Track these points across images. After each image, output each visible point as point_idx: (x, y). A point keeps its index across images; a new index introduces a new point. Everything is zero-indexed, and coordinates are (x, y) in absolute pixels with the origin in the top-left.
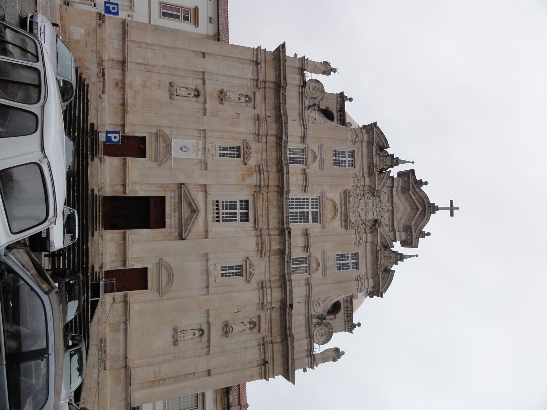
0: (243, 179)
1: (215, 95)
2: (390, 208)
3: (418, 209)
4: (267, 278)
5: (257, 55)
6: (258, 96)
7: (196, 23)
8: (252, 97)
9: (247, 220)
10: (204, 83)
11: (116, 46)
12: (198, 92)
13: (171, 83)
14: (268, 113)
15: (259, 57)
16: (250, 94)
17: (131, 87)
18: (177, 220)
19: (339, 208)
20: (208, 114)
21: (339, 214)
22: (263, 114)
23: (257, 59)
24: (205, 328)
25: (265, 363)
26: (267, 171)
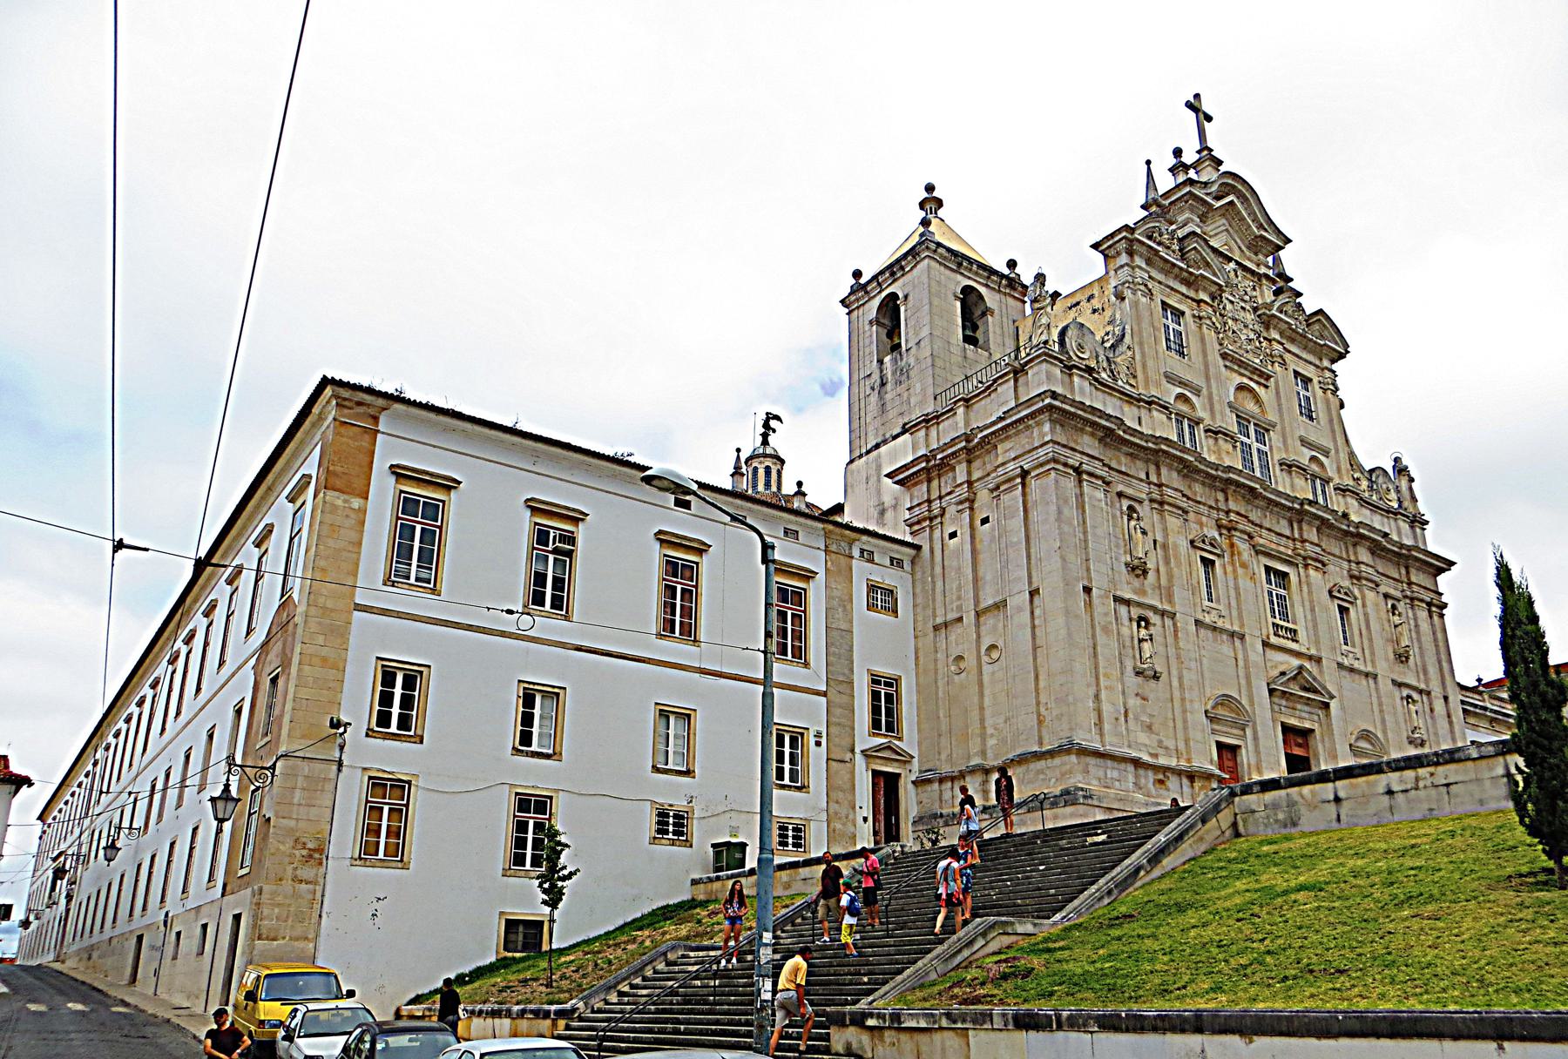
0: (1244, 565)
1: (1136, 583)
2: (1232, 265)
3: (1231, 203)
4: (1345, 565)
5: (1065, 465)
6: (1120, 488)
7: (808, 576)
8: (1125, 503)
9: (1285, 575)
10: (1128, 603)
11: (1115, 774)
12: (1141, 619)
13: (1138, 674)
14: (1143, 476)
15: (1070, 461)
16: (1125, 503)
17: (1155, 756)
18: (1306, 708)
19: (1245, 381)
20: (1167, 607)
21: (1253, 384)
22: (1145, 487)
23: (1072, 467)
24: (1405, 692)
25: (1429, 604)
26: (1227, 512)
